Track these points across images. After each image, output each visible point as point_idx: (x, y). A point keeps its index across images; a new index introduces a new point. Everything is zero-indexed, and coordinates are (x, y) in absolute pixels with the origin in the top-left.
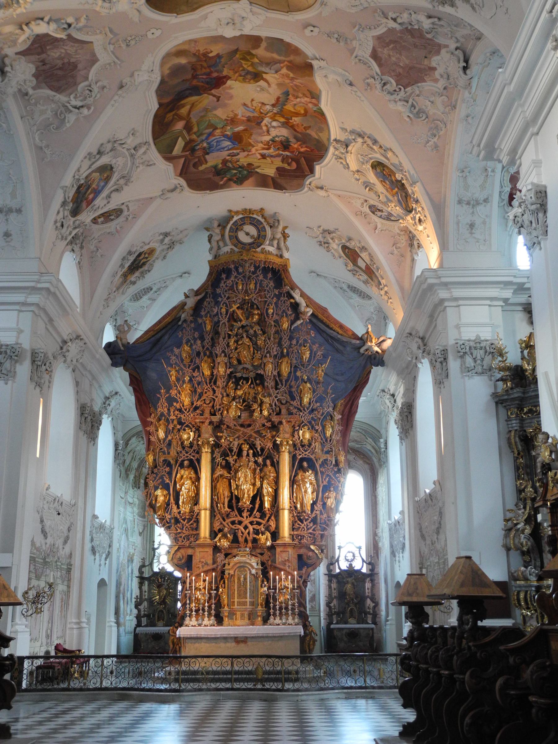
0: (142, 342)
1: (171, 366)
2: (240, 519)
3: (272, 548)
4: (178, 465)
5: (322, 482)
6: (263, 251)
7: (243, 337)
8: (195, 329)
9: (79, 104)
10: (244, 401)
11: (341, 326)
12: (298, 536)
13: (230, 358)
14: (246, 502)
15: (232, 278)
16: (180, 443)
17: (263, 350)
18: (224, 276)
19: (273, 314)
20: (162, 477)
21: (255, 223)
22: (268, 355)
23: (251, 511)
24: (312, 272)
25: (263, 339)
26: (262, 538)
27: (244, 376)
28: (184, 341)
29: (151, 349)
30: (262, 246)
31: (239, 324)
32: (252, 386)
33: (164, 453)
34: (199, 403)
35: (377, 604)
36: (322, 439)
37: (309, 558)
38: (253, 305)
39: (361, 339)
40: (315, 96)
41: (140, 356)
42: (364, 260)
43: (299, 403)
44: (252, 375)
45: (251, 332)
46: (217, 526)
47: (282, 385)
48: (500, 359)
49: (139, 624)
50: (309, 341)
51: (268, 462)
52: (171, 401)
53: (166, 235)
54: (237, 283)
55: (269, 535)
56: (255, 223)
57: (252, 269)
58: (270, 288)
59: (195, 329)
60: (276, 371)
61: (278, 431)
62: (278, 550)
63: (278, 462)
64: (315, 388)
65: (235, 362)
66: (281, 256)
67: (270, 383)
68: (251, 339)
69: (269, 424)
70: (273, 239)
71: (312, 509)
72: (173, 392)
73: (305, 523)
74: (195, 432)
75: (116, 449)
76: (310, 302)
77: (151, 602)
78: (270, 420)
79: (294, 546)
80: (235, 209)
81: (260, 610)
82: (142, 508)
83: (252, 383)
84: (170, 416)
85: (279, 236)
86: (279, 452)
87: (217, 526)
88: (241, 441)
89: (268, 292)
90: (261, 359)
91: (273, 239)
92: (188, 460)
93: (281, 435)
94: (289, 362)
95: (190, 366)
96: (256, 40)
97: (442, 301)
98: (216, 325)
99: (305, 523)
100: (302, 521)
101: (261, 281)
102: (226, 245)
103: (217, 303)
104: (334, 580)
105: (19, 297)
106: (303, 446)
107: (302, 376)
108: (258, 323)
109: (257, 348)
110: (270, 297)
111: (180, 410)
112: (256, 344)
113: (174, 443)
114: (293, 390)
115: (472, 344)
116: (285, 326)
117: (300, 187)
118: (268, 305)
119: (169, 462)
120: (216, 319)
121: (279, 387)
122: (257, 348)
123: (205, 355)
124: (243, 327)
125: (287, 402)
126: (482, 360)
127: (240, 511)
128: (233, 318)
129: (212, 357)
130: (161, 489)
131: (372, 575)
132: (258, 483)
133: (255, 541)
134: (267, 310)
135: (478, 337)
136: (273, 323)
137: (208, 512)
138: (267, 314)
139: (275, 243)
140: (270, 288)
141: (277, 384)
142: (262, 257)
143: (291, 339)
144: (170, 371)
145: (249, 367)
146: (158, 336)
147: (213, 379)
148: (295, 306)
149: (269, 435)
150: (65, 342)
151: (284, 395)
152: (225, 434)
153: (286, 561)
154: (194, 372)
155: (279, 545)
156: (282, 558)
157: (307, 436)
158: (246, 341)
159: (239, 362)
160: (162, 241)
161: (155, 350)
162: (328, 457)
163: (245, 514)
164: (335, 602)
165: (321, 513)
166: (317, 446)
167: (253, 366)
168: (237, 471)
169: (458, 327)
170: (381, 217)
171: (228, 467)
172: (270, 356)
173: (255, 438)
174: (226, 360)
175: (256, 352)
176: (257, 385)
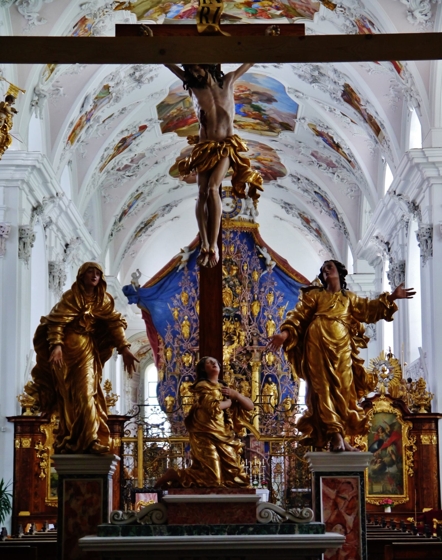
0: (151, 287)
1: (174, 307)
3: (248, 438)
4: (181, 380)
5: (282, 392)
6: (240, 220)
7: (225, 287)
11: (298, 275)
16: (182, 364)
17: (240, 296)
19: (247, 270)
22: (244, 301)
24: (276, 217)
25: (240, 288)
27: (227, 315)
28: (183, 289)
30: (239, 215)
32: (232, 322)
36: (282, 361)
38: (232, 262)
41: (149, 296)
43: (266, 335)
44: (232, 314)
45: (232, 283)
47: (254, 321)
50: (273, 289)
52: (175, 333)
57: (232, 236)
58: (245, 250)
60: (250, 313)
62: (251, 439)
64: (278, 324)
66: (253, 222)
67: (245, 321)
68: (231, 288)
69: (244, 352)
72: (176, 327)
73: (270, 420)
74: (192, 357)
78: (245, 349)
82: (134, 394)
83: (232, 320)
84: (174, 344)
86: (252, 372)
89: (244, 253)
90: (239, 303)
91: (247, 209)
92: (187, 376)
93: (253, 360)
94: (259, 305)
95: (187, 307)
99: (270, 420)
101: (239, 245)
106: (269, 366)
107: (268, 316)
108: (236, 276)
109: (236, 295)
110: (245, 257)
111: (181, 340)
112: (235, 291)
113: (178, 364)
114: (262, 325)
118: (244, 263)
119: (174, 377)
121: (251, 323)
125: (257, 334)
130: (169, 396)
134: (243, 267)
136: (247, 276)
138: (243, 270)
139: (248, 212)
140: (245, 250)
141: (250, 321)
142: (238, 224)
143: (260, 287)
144: (173, 312)
146: (162, 282)
148: (263, 260)
149: (245, 359)
151: (255, 329)
153: (257, 446)
154: (190, 312)
156: (254, 444)
157: (272, 358)
161: (160, 292)
162: (286, 373)
166: (279, 366)
167: (233, 308)
172: (246, 301)
175: (235, 297)
176: (236, 321)
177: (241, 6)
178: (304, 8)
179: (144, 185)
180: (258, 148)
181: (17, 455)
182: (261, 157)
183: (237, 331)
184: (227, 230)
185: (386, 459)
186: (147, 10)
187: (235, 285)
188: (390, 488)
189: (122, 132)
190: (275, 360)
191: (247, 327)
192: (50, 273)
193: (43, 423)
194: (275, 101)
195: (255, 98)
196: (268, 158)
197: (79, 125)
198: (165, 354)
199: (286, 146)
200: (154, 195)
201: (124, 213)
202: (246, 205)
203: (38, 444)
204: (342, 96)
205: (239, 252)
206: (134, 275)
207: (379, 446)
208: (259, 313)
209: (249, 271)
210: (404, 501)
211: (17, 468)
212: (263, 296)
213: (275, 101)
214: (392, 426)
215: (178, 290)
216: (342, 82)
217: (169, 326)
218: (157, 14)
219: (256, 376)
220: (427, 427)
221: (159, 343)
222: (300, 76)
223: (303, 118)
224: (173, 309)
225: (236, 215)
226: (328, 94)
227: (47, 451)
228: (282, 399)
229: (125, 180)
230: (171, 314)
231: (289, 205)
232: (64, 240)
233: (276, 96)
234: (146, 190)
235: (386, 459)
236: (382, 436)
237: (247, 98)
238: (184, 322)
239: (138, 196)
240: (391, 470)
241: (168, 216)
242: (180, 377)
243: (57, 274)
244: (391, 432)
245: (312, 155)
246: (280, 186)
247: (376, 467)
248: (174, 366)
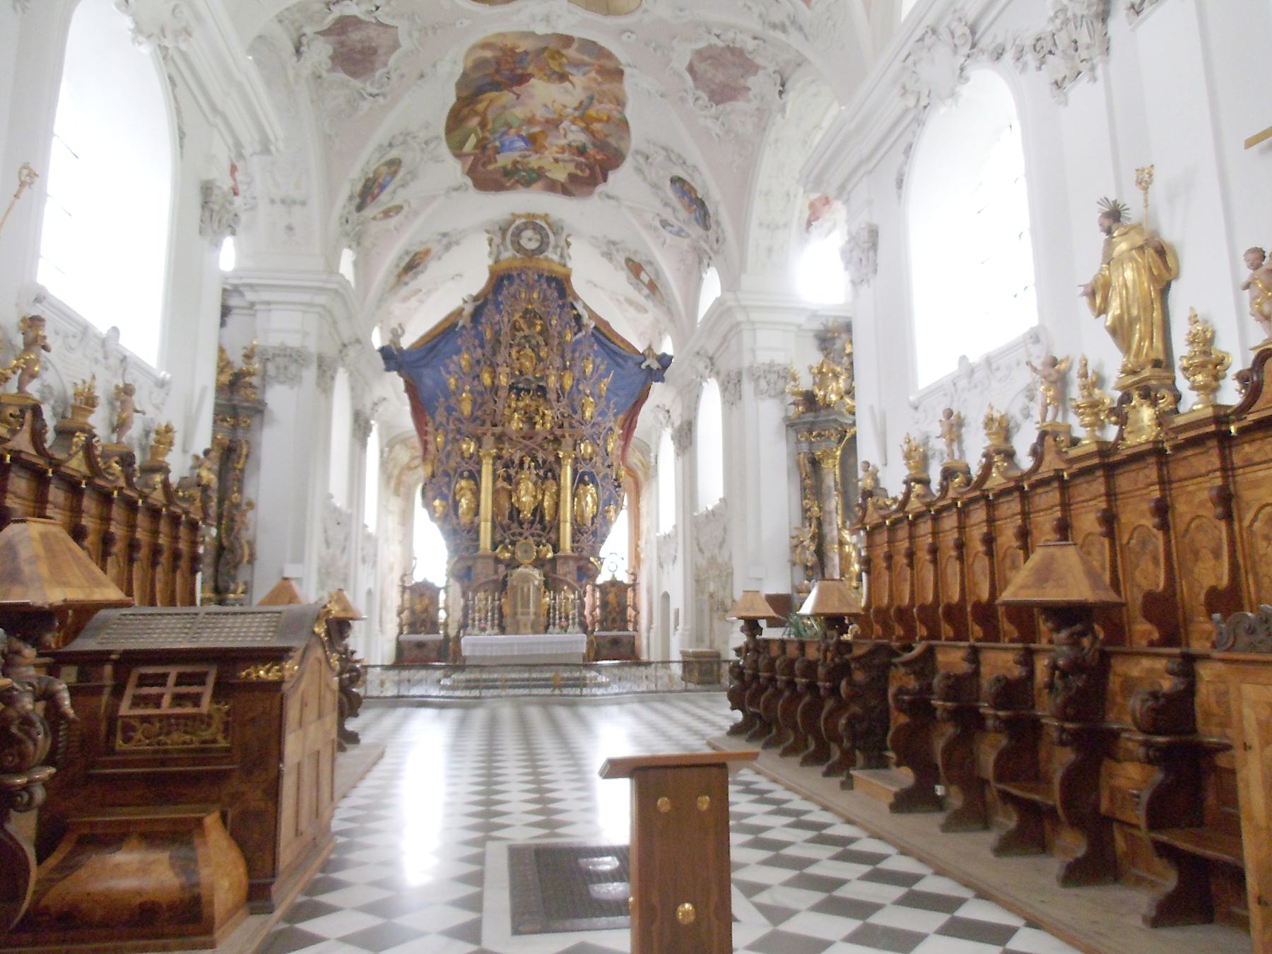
1: (449, 373)
2: (521, 530)
3: (554, 560)
6: (547, 259)
8: (476, 337)
9: (375, 91)
10: (526, 413)
11: (623, 340)
12: (578, 548)
13: (512, 368)
14: (527, 514)
15: (515, 286)
18: (506, 282)
20: (440, 488)
21: (537, 229)
23: (532, 523)
29: (425, 357)
30: (545, 254)
31: (522, 334)
33: (442, 463)
34: (479, 413)
35: (638, 612)
37: (589, 569)
38: (536, 314)
40: (620, 102)
44: (534, 386)
45: (534, 342)
46: (498, 538)
48: (793, 383)
49: (401, 633)
51: (549, 474)
53: (444, 235)
54: (520, 292)
55: (550, 547)
56: (537, 229)
57: (536, 277)
59: (476, 337)
61: (560, 444)
62: (559, 562)
63: (559, 476)
65: (517, 373)
66: (565, 266)
67: (552, 396)
69: (551, 437)
70: (556, 247)
71: (593, 523)
72: (453, 401)
75: (382, 456)
76: (593, 315)
77: (413, 612)
78: (552, 433)
80: (518, 212)
81: (543, 619)
85: (563, 243)
86: (560, 466)
87: (498, 538)
88: (523, 454)
91: (556, 247)
96: (568, 40)
97: (738, 324)
98: (497, 334)
100: (580, 532)
102: (506, 250)
104: (597, 590)
105: (306, 297)
106: (584, 460)
108: (541, 333)
111: (459, 420)
113: (454, 454)
115: (767, 368)
116: (568, 337)
117: (590, 193)
120: (497, 327)
122: (540, 359)
123: (485, 363)
124: (525, 337)
126: (775, 383)
127: (521, 524)
131: (634, 586)
132: (540, 497)
134: (550, 321)
135: (772, 361)
136: (556, 334)
137: (489, 524)
139: (559, 250)
141: (559, 397)
142: (545, 265)
145: (530, 377)
146: (436, 340)
147: (495, 389)
148: (578, 318)
149: (551, 448)
150: (345, 346)
152: (507, 445)
155: (560, 557)
157: (589, 450)
158: (528, 351)
159: (521, 372)
160: (440, 241)
163: (525, 526)
164: (598, 611)
165: (601, 526)
168: (518, 483)
169: (753, 351)
170: (670, 232)
171: (508, 479)
173: (537, 451)
174: (508, 370)
176: (539, 397)
180: (593, 74)
183: (541, 409)
184: (529, 268)
190: (594, 452)
191: (554, 404)
198: (435, 439)
202: (556, 241)
205: (545, 299)
208: (572, 387)
209: (559, 328)
217: (442, 399)
219: (568, 471)
224: (448, 376)
225: (541, 253)
228: (603, 507)
229: (365, 106)
231: (614, 243)
238: (464, 395)
242: (455, 472)
246: (609, 197)
248: (448, 455)
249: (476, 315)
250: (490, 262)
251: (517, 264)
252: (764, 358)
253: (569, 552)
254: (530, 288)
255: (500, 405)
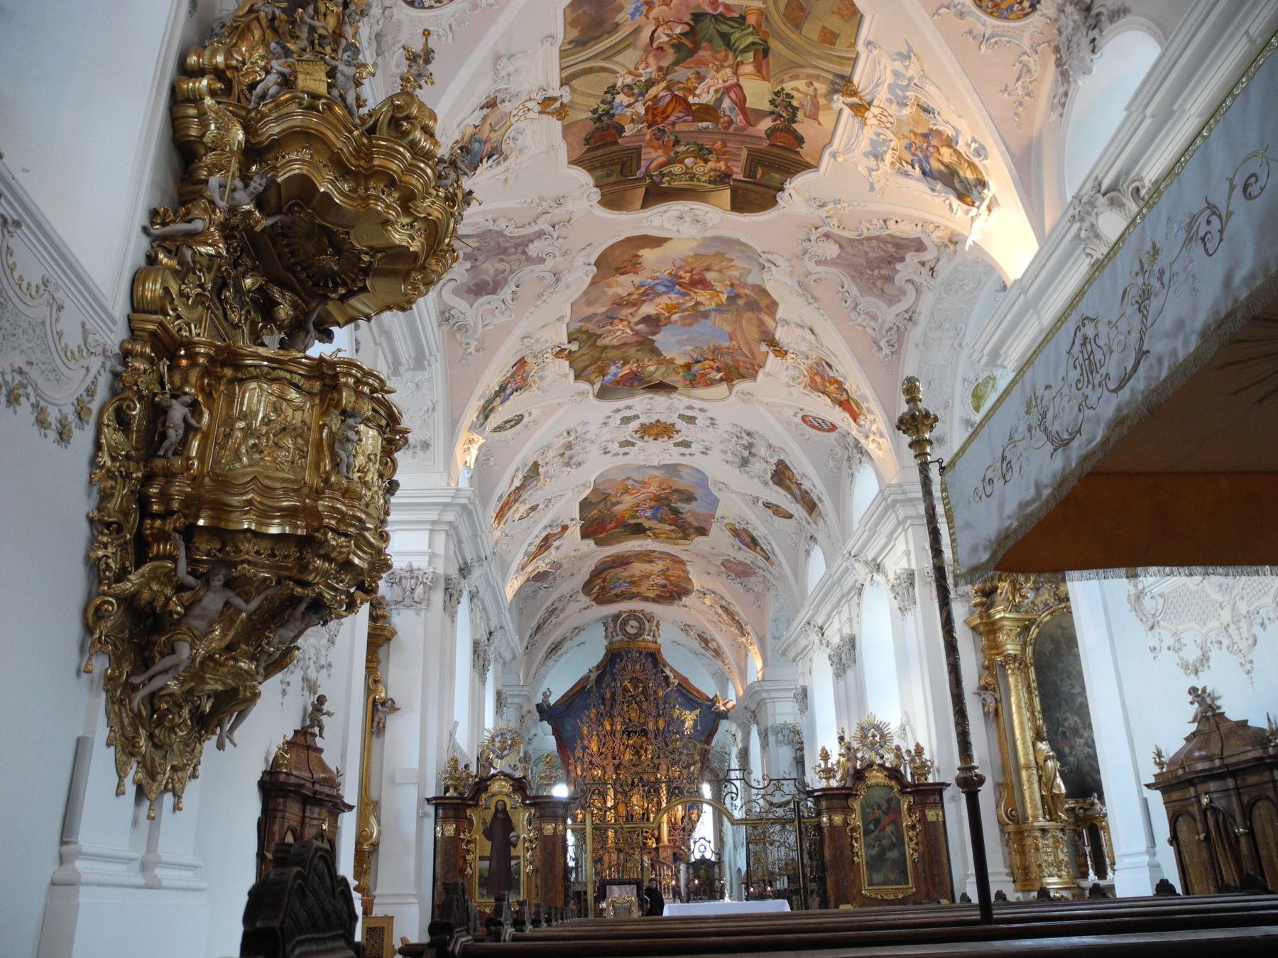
3: (657, 849)
6: (644, 640)
11: (698, 692)
21: (638, 619)
26: (650, 842)
34: (603, 750)
39: (712, 701)
42: (713, 645)
44: (639, 729)
45: (638, 699)
52: (585, 748)
56: (638, 619)
61: (658, 769)
62: (661, 850)
66: (656, 642)
67: (651, 736)
76: (677, 674)
79: (671, 847)
85: (654, 628)
91: (650, 630)
96: (654, 551)
98: (613, 694)
103: (614, 680)
108: (642, 693)
109: (642, 711)
122: (642, 711)
128: (626, 690)
129: (611, 717)
131: (719, 863)
133: (645, 844)
143: (665, 703)
147: (613, 733)
148: (667, 678)
158: (635, 705)
159: (630, 720)
169: (774, 715)
171: (625, 793)
177: (680, 370)
178: (748, 366)
179: (559, 600)
181: (439, 845)
182: (670, 573)
183: (645, 745)
185: (886, 842)
186: (586, 368)
187: (641, 701)
188: (893, 877)
189: (546, 527)
191: (653, 741)
192: (475, 652)
193: (469, 806)
194: (695, 499)
195: (675, 497)
196: (677, 573)
197: (507, 503)
199: (697, 555)
200: (567, 612)
201: (539, 628)
203: (464, 832)
204: (772, 478)
206: (544, 694)
207: (876, 827)
210: (910, 892)
211: (438, 861)
212: (667, 711)
213: (695, 499)
214: (889, 801)
215: (587, 707)
216: (774, 460)
218: (595, 375)
220: (931, 800)
221: (569, 759)
222: (727, 462)
223: (722, 518)
226: (756, 480)
227: (475, 841)
229: (542, 593)
230: (580, 730)
232: (488, 626)
233: (698, 493)
234: (560, 605)
235: (886, 842)
236: (878, 813)
237: (667, 498)
239: (552, 612)
240: (893, 855)
241: (578, 640)
243: (482, 653)
244: (888, 809)
245: (722, 564)
247: (875, 851)
249: (599, 679)
250: (605, 643)
251: (625, 645)
252: (780, 720)
253: (666, 843)
254: (634, 663)
255: (617, 741)
